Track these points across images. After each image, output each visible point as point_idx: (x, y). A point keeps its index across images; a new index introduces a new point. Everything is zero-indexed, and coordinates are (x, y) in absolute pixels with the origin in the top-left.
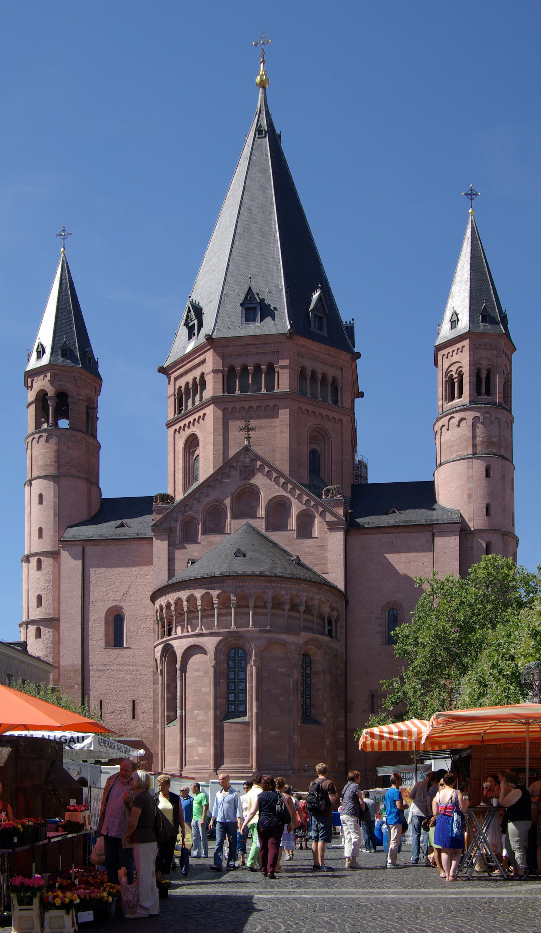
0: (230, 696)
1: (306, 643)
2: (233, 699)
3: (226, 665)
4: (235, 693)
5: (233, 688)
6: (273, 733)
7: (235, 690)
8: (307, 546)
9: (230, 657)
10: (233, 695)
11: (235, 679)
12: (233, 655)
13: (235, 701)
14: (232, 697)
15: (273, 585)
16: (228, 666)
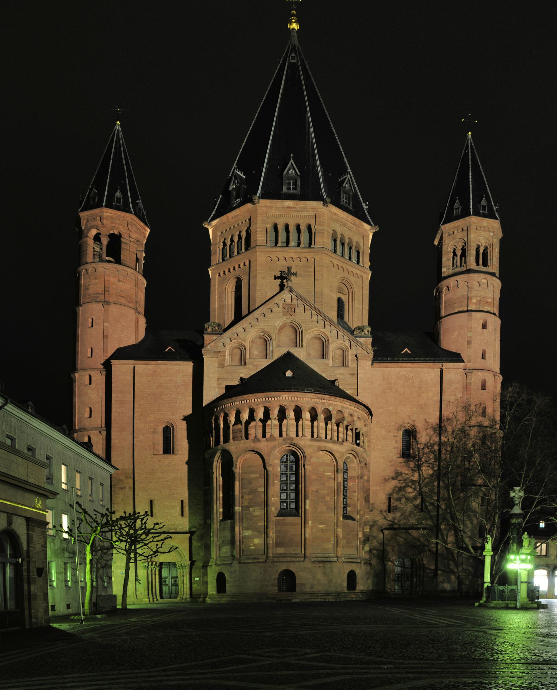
0: (282, 495)
1: (347, 452)
2: (285, 498)
3: (279, 468)
4: (287, 493)
5: (285, 488)
6: (321, 526)
7: (287, 490)
8: (340, 374)
9: (283, 462)
10: (285, 494)
11: (287, 480)
12: (285, 460)
13: (287, 499)
14: (284, 496)
15: (323, 401)
16: (281, 469)
